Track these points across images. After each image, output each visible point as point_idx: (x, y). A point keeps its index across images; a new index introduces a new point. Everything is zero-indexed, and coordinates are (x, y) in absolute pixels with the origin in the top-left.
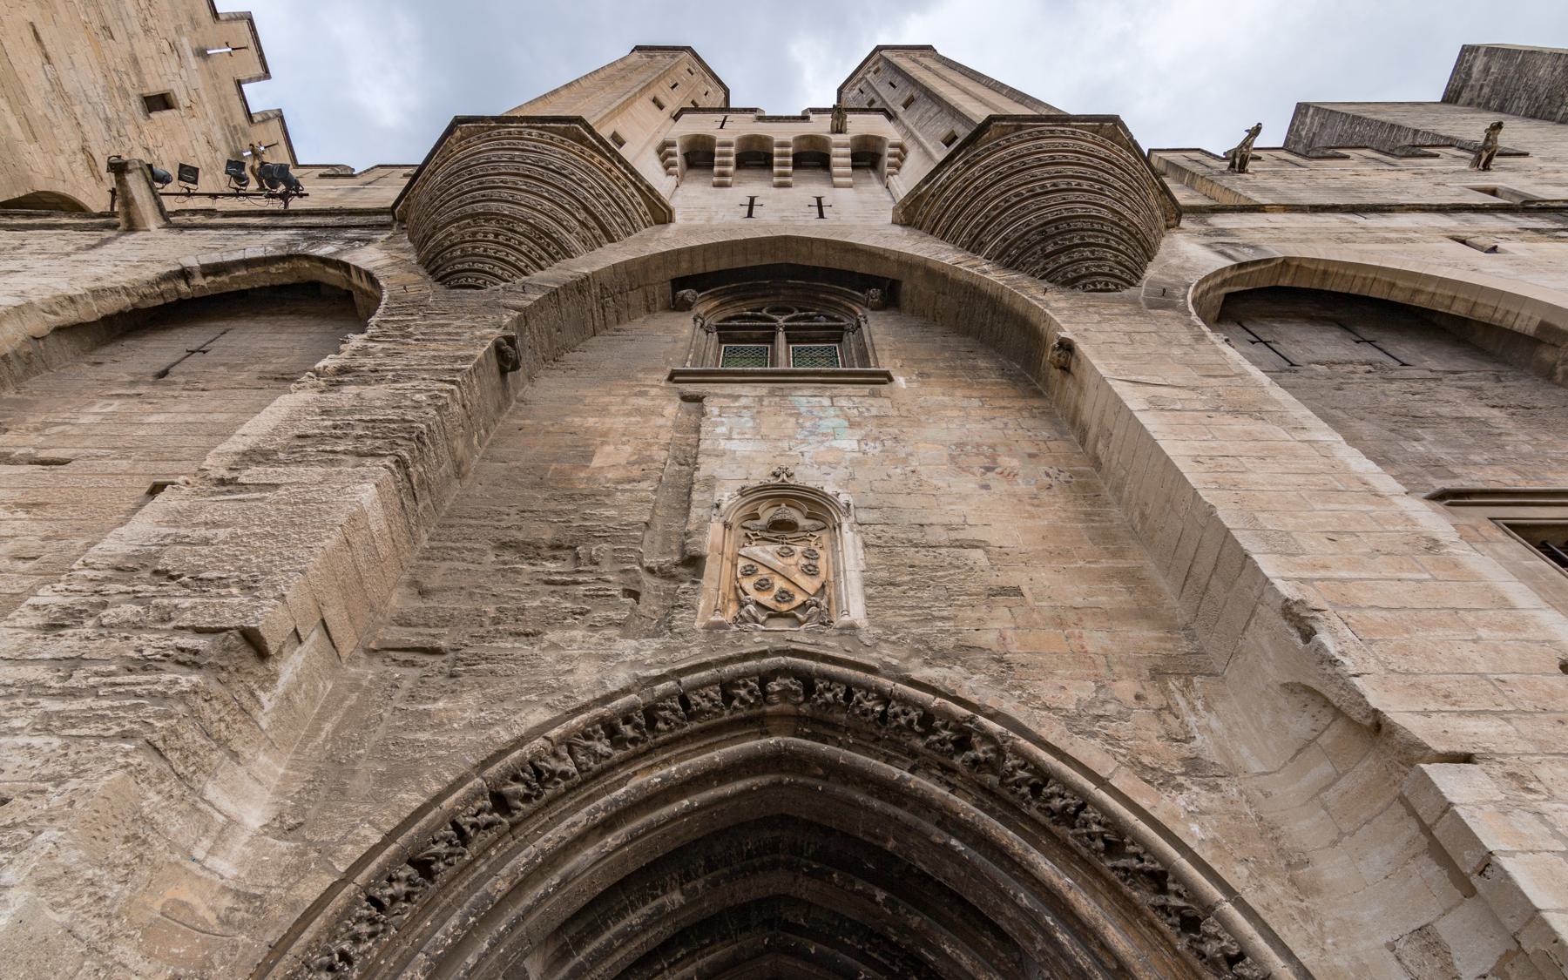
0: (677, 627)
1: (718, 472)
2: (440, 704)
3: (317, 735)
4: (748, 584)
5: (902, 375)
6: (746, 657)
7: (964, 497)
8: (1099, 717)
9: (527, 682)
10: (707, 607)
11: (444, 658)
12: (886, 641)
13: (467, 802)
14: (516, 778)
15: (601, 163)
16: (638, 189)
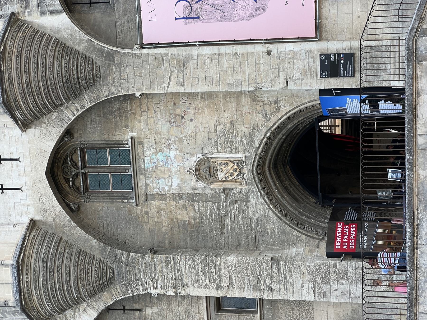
0: (247, 192)
1: (189, 187)
2: (269, 231)
3: (277, 249)
4: (231, 178)
5: (128, 133)
6: (254, 178)
7: (196, 127)
8: (266, 115)
9: (263, 217)
10: (240, 186)
11: (257, 234)
12: (249, 151)
13: (288, 220)
14: (282, 214)
15: (30, 250)
16: (30, 234)
